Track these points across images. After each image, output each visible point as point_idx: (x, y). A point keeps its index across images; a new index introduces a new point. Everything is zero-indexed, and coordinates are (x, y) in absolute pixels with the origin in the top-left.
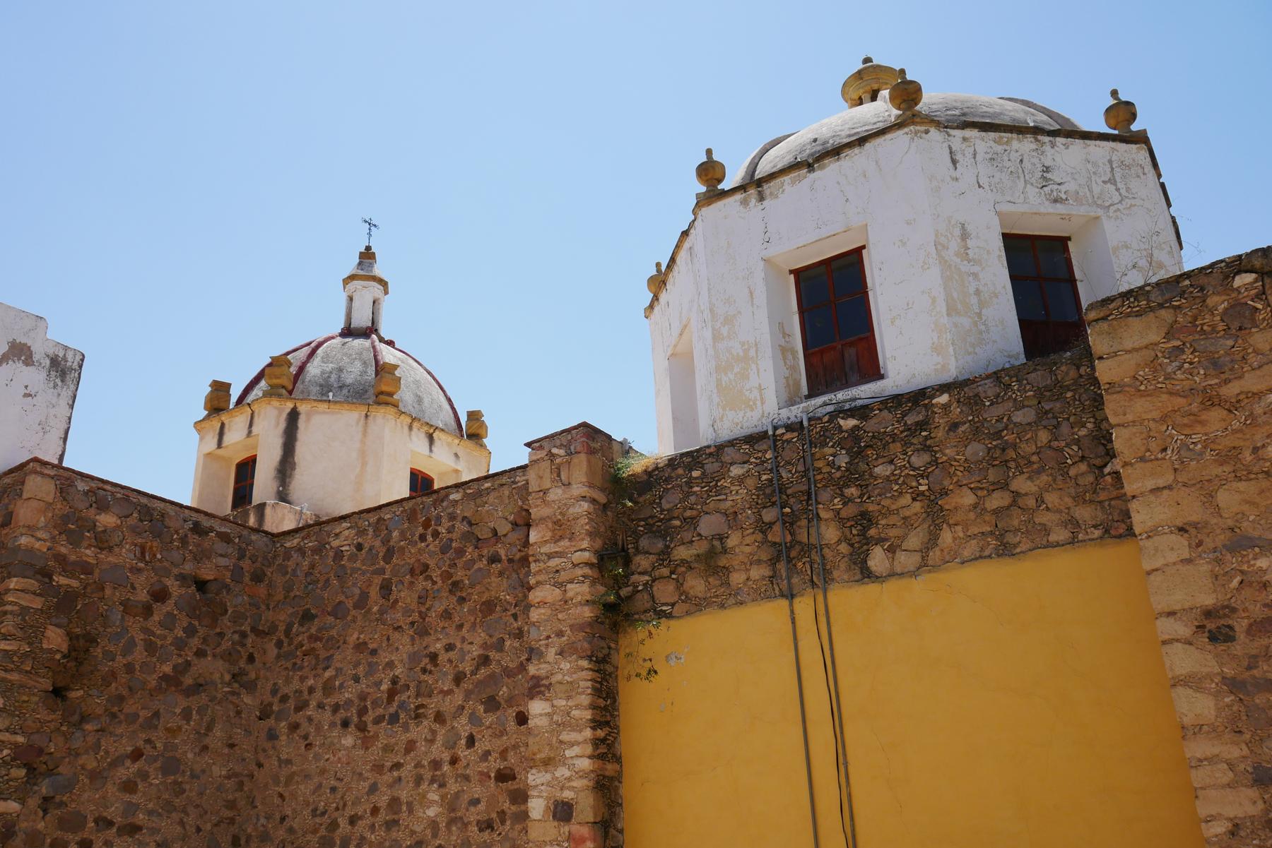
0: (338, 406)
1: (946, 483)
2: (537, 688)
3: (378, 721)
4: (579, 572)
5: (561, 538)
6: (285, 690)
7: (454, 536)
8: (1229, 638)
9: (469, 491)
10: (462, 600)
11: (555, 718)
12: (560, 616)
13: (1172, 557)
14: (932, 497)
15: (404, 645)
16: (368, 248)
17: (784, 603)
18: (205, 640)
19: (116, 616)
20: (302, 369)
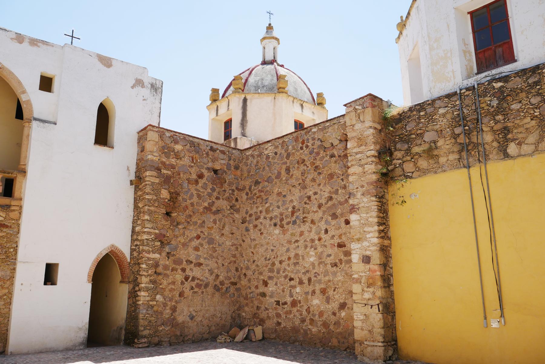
0: (263, 95)
2: (353, 209)
3: (288, 223)
4: (370, 160)
6: (251, 212)
7: (315, 147)
9: (320, 127)
10: (320, 174)
11: (362, 221)
12: (362, 179)
14: (542, 118)
15: (297, 193)
16: (270, 24)
17: (465, 170)
18: (219, 193)
19: (185, 185)
20: (246, 80)
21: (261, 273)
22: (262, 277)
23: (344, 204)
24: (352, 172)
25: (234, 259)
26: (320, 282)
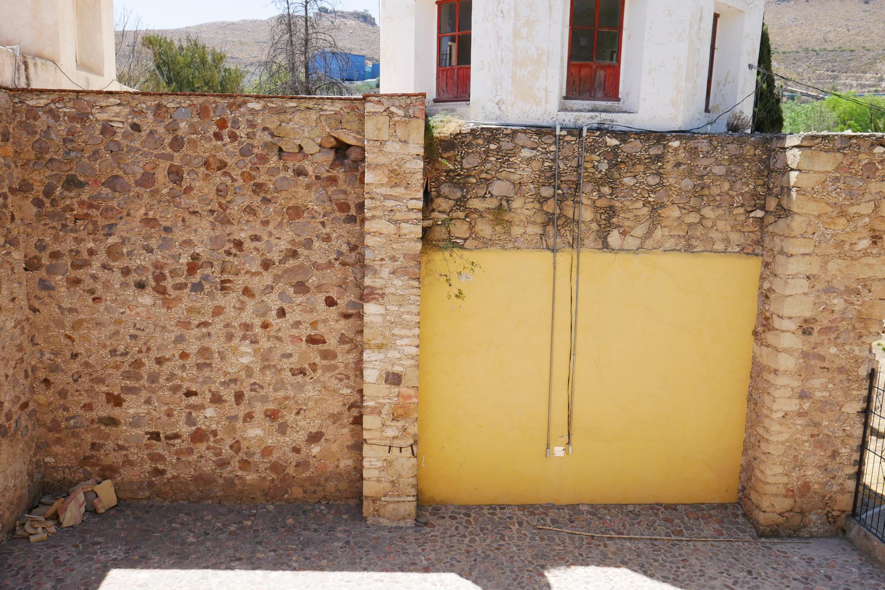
1: (665, 200)
3: (179, 287)
5: (396, 185)
6: (56, 247)
7: (255, 143)
8: (810, 334)
10: (266, 201)
11: (388, 318)
12: (394, 246)
13: (800, 291)
17: (550, 254)
21: (101, 381)
22: (105, 389)
23: (322, 269)
25: (19, 355)
26: (264, 399)
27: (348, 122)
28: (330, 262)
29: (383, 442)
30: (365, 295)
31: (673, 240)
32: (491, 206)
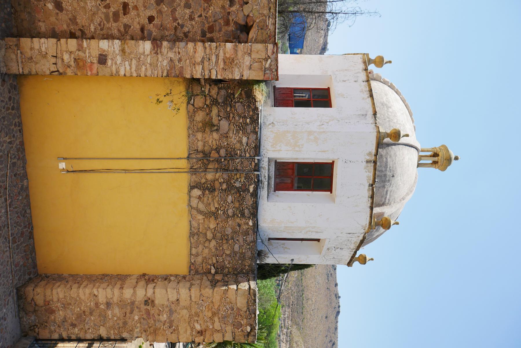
1: (220, 220)
4: (207, 73)
5: (225, 62)
8: (145, 304)
11: (142, 56)
12: (188, 61)
13: (170, 296)
17: (186, 155)
24: (197, 48)
27: (262, 33)
28: (177, 20)
29: (59, 52)
30: (156, 42)
31: (197, 225)
32: (213, 120)
